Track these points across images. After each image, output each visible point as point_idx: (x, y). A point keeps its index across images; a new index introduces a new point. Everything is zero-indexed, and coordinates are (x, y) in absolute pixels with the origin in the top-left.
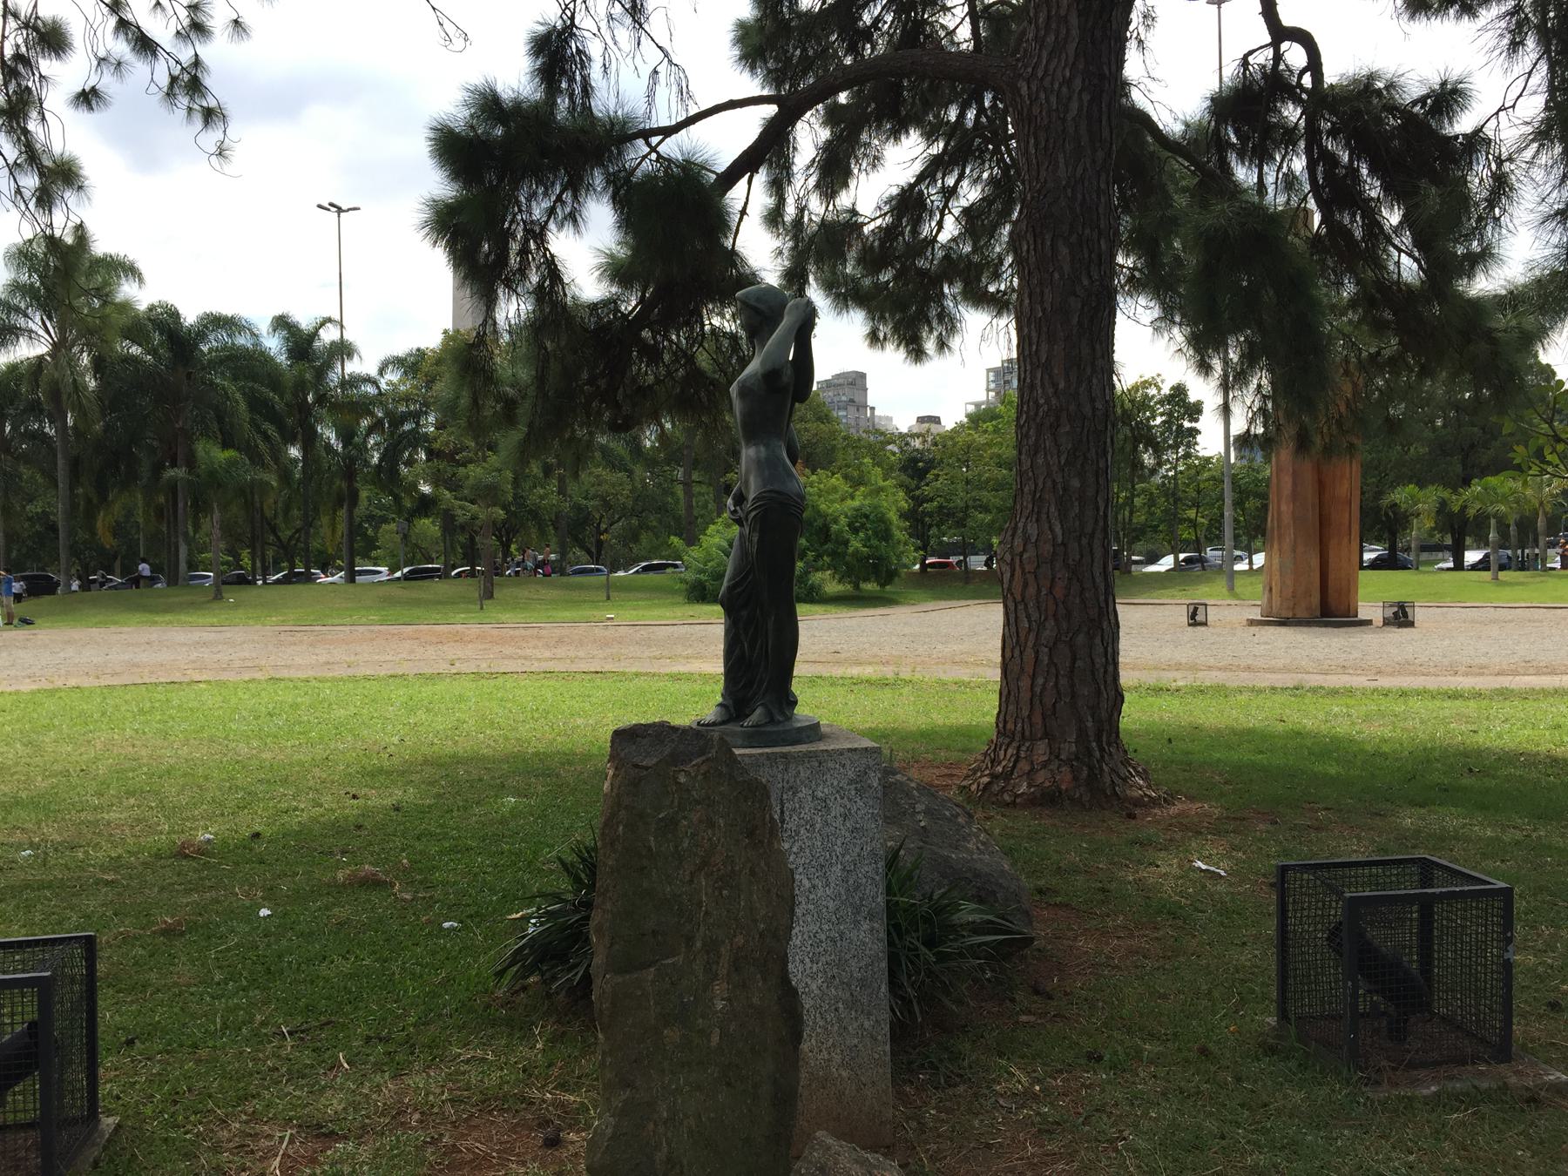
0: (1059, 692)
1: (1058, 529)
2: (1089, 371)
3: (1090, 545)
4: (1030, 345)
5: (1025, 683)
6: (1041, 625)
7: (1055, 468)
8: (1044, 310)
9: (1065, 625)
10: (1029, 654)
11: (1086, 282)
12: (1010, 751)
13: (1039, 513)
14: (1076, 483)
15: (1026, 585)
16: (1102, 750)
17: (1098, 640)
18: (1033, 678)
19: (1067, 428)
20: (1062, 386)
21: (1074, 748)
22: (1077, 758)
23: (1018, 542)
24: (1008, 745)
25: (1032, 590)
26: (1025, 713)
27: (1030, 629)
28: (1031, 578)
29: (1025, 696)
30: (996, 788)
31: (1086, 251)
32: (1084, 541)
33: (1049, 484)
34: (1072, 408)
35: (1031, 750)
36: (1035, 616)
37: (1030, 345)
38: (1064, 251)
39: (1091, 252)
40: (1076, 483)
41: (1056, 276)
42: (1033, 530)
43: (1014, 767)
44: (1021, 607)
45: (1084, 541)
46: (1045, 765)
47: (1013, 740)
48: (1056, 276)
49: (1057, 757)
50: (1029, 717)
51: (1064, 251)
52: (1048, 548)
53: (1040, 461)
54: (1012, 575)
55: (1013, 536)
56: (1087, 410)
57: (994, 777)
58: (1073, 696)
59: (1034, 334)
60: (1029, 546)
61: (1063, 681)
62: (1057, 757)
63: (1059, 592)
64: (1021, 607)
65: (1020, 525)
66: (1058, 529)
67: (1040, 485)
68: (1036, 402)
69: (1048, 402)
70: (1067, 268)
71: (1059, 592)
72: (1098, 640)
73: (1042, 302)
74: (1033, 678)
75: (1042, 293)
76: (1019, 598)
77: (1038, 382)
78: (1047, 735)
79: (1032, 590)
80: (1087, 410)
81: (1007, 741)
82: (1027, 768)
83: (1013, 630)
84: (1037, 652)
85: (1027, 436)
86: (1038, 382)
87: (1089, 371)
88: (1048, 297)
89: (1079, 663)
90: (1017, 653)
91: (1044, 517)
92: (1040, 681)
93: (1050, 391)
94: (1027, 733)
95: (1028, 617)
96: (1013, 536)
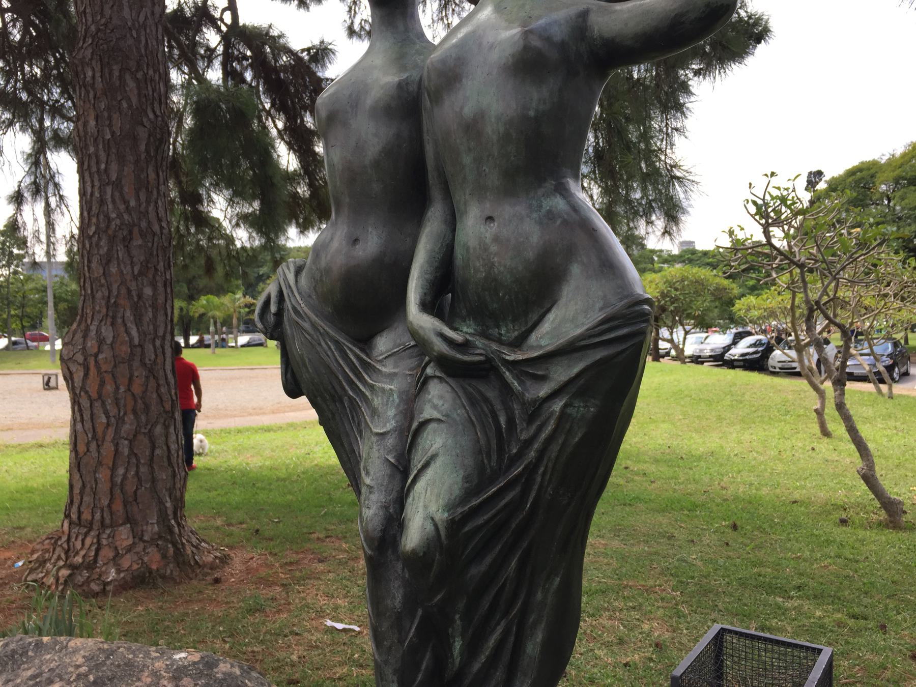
0: (140, 480)
1: (134, 332)
2: (155, 193)
3: (163, 347)
4: (98, 163)
5: (103, 475)
6: (120, 420)
7: (128, 277)
8: (113, 133)
9: (143, 418)
10: (108, 448)
11: (151, 116)
12: (88, 541)
13: (114, 318)
14: (148, 291)
15: (102, 384)
16: (179, 524)
17: (172, 430)
18: (113, 469)
19: (140, 242)
20: (133, 203)
21: (156, 528)
22: (160, 537)
23: (92, 344)
24: (86, 535)
25: (109, 388)
26: (105, 502)
27: (108, 425)
28: (108, 377)
29: (104, 487)
30: (80, 579)
31: (150, 88)
32: (158, 343)
33: (123, 291)
34: (144, 224)
35: (112, 536)
36: (113, 411)
37: (98, 163)
38: (131, 84)
39: (154, 91)
40: (148, 291)
41: (125, 105)
42: (107, 333)
43: (96, 555)
44: (97, 404)
45: (158, 343)
46: (129, 549)
47: (90, 529)
48: (125, 105)
49: (141, 539)
50: (109, 506)
51: (131, 84)
52: (126, 349)
53: (113, 269)
54: (86, 375)
55: (85, 337)
56: (156, 228)
57: (74, 568)
58: (154, 481)
59: (103, 155)
60: (105, 347)
61: (144, 470)
62: (141, 539)
63: (137, 389)
64: (97, 404)
65: (93, 328)
66: (134, 332)
67: (115, 292)
68: (107, 217)
69: (120, 216)
70: (134, 100)
71: (137, 389)
72: (172, 430)
73: (110, 126)
74: (113, 469)
75: (110, 118)
76: (94, 395)
77: (108, 196)
78: (129, 519)
79: (109, 388)
80: (156, 228)
81: (84, 530)
82: (111, 555)
83: (88, 425)
84: (117, 445)
85: (98, 245)
86: (108, 196)
87: (155, 193)
88: (117, 123)
89: (158, 452)
90: (93, 446)
91: (120, 321)
92: (121, 471)
93: (122, 207)
94: (108, 521)
95: (106, 413)
96: (85, 337)
